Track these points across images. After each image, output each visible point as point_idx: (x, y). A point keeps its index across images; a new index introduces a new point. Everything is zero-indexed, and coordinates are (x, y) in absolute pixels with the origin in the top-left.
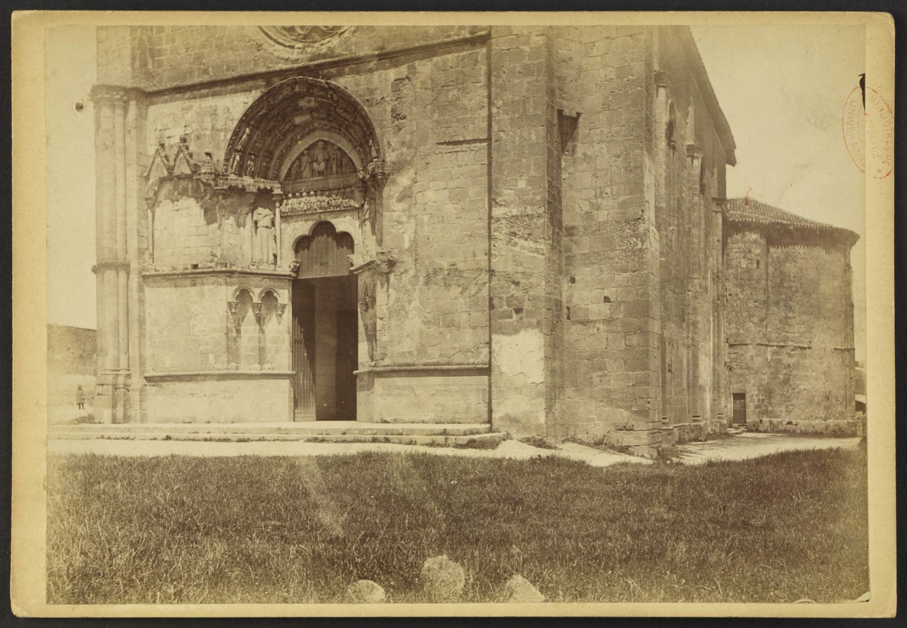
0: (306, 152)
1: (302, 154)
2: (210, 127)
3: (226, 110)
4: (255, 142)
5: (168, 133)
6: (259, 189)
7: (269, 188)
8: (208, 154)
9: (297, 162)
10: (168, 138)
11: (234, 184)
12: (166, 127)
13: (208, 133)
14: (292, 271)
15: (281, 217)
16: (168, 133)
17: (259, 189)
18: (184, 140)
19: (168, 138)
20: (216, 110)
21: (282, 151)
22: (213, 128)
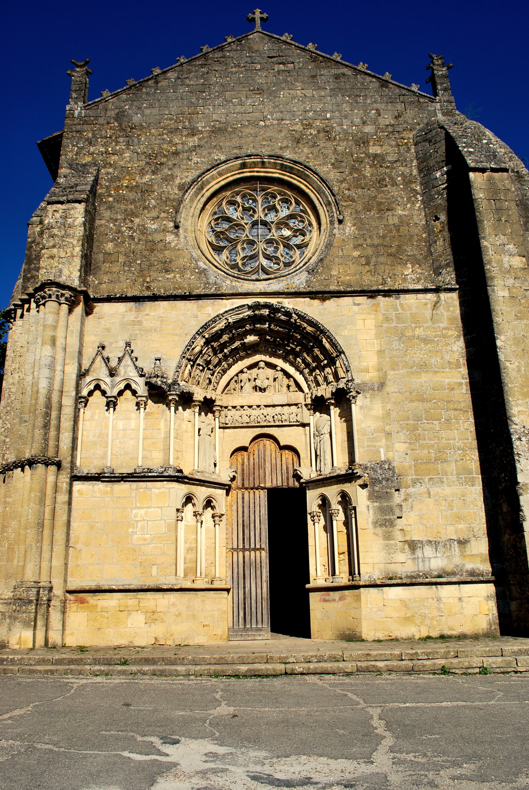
0: (245, 370)
1: (242, 372)
6: (205, 398)
7: (214, 399)
9: (236, 378)
15: (220, 428)
17: (205, 398)
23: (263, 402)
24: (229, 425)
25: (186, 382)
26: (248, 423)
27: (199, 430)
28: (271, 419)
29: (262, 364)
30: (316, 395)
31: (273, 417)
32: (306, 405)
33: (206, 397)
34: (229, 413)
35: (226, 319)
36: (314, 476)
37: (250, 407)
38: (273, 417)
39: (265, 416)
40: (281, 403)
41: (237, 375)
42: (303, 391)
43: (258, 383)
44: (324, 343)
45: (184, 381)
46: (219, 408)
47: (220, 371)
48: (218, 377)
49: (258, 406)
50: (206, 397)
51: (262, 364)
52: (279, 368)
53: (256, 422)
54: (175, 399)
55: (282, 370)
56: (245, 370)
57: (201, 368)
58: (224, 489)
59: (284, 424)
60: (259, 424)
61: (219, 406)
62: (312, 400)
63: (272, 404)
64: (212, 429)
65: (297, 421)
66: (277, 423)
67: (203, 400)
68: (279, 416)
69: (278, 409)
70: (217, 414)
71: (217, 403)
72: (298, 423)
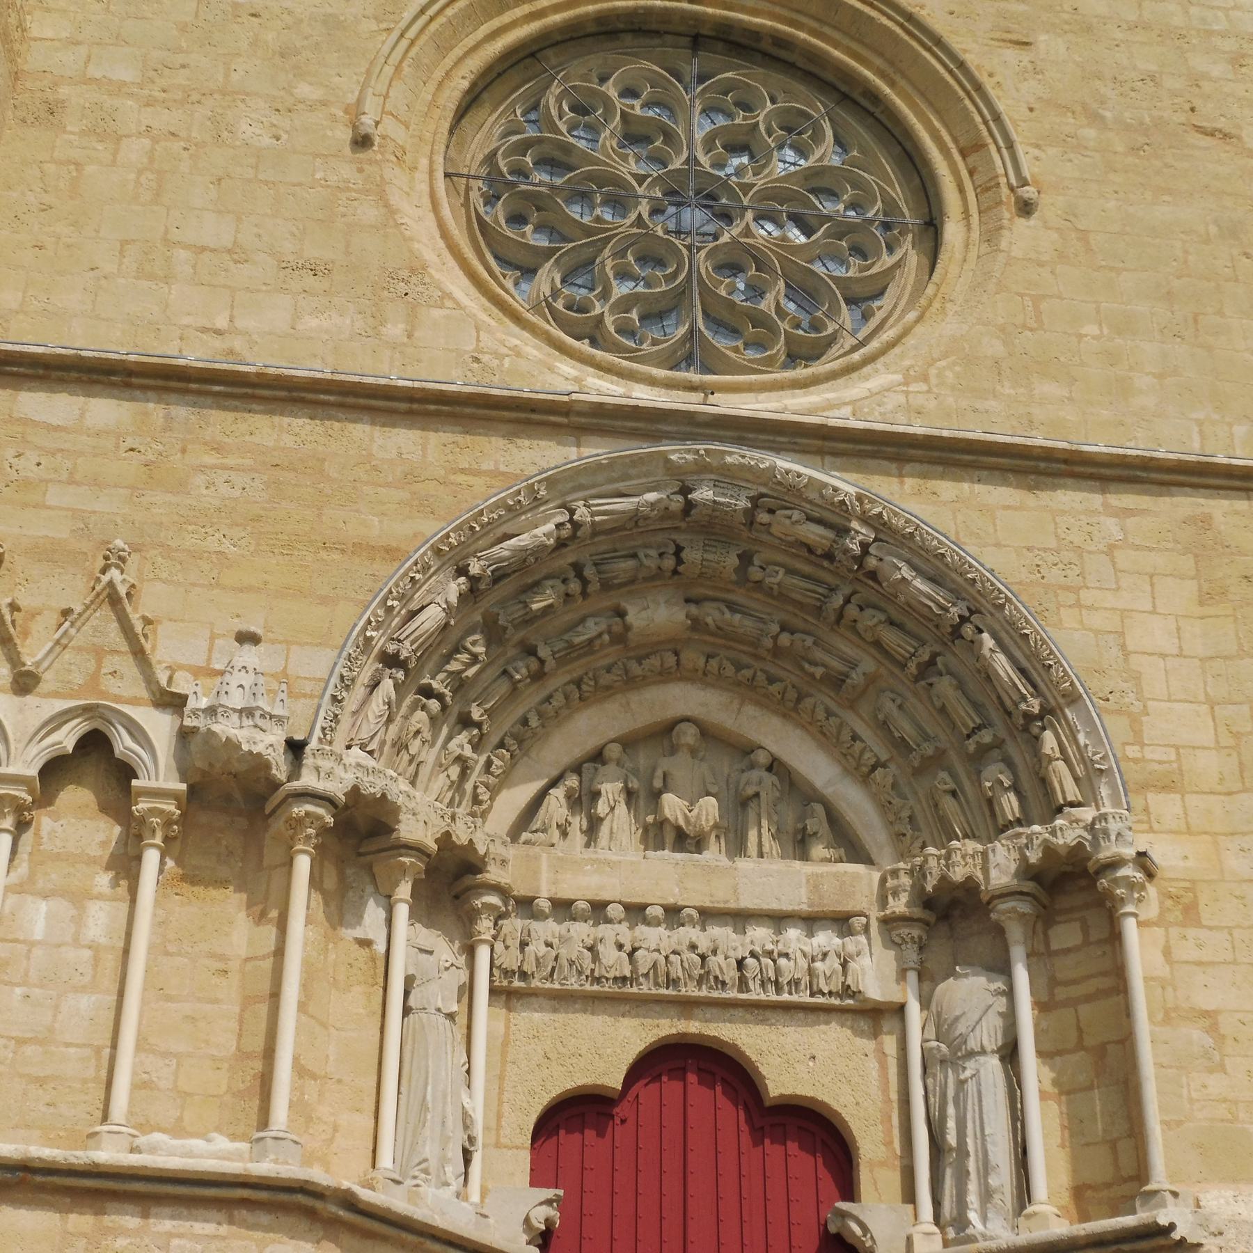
15: (493, 992)
17: (445, 840)
21: (525, 722)
23: (695, 895)
25: (371, 753)
27: (409, 982)
28: (731, 974)
29: (689, 735)
30: (944, 879)
31: (740, 964)
33: (447, 835)
35: (563, 506)
38: (740, 964)
40: (774, 905)
43: (673, 805)
44: (986, 652)
45: (362, 747)
46: (494, 899)
50: (447, 835)
51: (689, 735)
53: (662, 979)
54: (320, 818)
56: (614, 751)
57: (434, 704)
60: (671, 992)
63: (732, 905)
65: (846, 991)
66: (756, 994)
68: (766, 961)
69: (760, 935)
70: (485, 926)
71: (493, 874)
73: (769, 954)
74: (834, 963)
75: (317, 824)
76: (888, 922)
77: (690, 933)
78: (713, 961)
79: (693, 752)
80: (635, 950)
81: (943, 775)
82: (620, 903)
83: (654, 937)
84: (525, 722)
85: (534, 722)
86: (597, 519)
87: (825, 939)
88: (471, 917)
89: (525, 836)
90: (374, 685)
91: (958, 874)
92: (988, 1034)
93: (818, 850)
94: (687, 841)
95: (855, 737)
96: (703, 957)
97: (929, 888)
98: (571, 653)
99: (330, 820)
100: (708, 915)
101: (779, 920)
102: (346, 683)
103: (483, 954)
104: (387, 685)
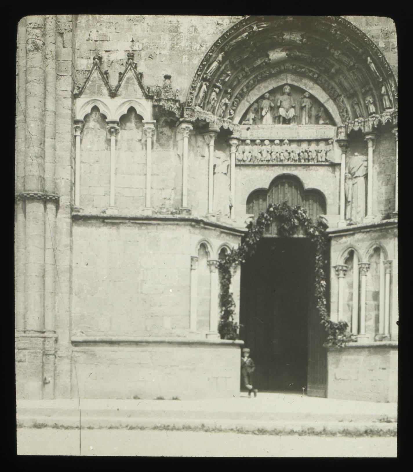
1: (263, 97)
2: (169, 46)
3: (192, 29)
4: (223, 72)
5: (106, 46)
6: (222, 128)
7: (231, 129)
8: (167, 77)
10: (106, 51)
11: (202, 117)
12: (104, 39)
13: (165, 52)
14: (247, 227)
16: (106, 46)
17: (222, 128)
18: (131, 56)
19: (106, 51)
20: (177, 27)
21: (242, 90)
22: (172, 48)
24: (247, 163)
25: (201, 107)
26: (269, 161)
27: (215, 166)
29: (287, 89)
31: (299, 155)
32: (338, 141)
33: (222, 127)
34: (247, 148)
36: (343, 225)
37: (272, 141)
39: (289, 153)
40: (309, 138)
41: (257, 101)
42: (334, 124)
43: (282, 112)
45: (199, 106)
47: (238, 96)
48: (235, 103)
49: (282, 141)
50: (222, 127)
52: (307, 95)
53: (279, 160)
54: (189, 128)
55: (312, 97)
57: (217, 90)
58: (239, 236)
59: (310, 163)
60: (281, 163)
61: (236, 139)
62: (347, 135)
63: (298, 139)
64: (228, 166)
65: (326, 160)
66: (303, 162)
67: (219, 130)
68: (306, 154)
69: (305, 146)
71: (235, 135)
72: (327, 163)
73: (306, 151)
74: (323, 153)
75: (189, 129)
76: (338, 141)
77: (286, 147)
78: (292, 154)
79: (289, 94)
80: (272, 152)
81: (356, 99)
82: (268, 140)
83: (277, 149)
84: (242, 90)
85: (245, 90)
86: (260, 29)
87: (322, 146)
88: (230, 146)
89: (244, 122)
90: (201, 86)
91: (356, 129)
92: (361, 172)
93: (321, 122)
94: (286, 121)
95: (333, 88)
96: (289, 153)
97: (349, 133)
98: (253, 70)
99: (192, 128)
100: (291, 141)
101: (309, 141)
102: (194, 88)
103: (233, 156)
104: (204, 87)
